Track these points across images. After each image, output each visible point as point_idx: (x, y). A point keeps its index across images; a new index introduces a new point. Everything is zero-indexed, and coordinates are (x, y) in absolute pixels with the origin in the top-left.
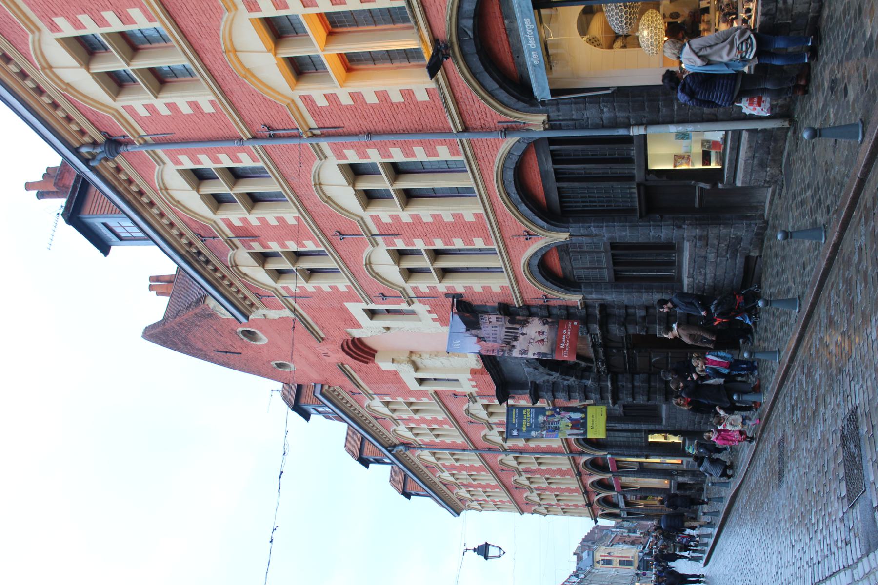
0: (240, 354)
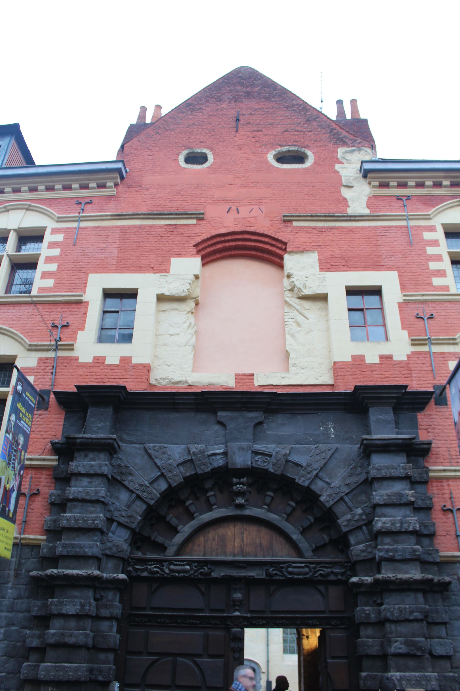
0: (237, 131)
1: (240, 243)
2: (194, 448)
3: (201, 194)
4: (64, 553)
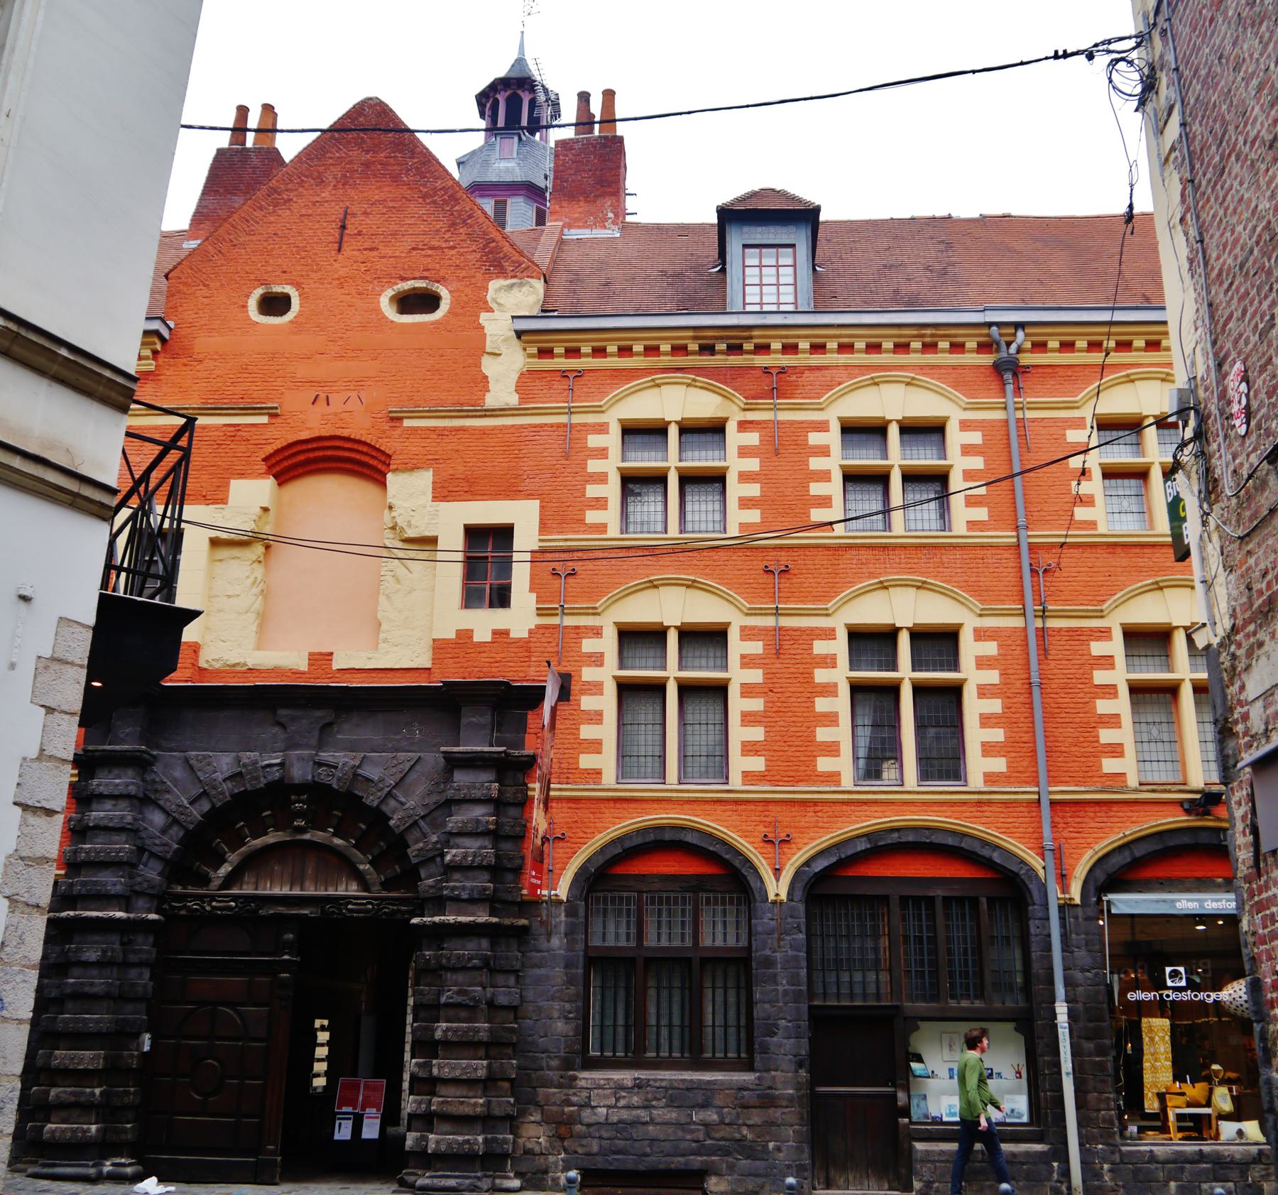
0: (339, 250)
1: (329, 453)
2: (247, 757)
3: (278, 370)
4: (84, 892)
